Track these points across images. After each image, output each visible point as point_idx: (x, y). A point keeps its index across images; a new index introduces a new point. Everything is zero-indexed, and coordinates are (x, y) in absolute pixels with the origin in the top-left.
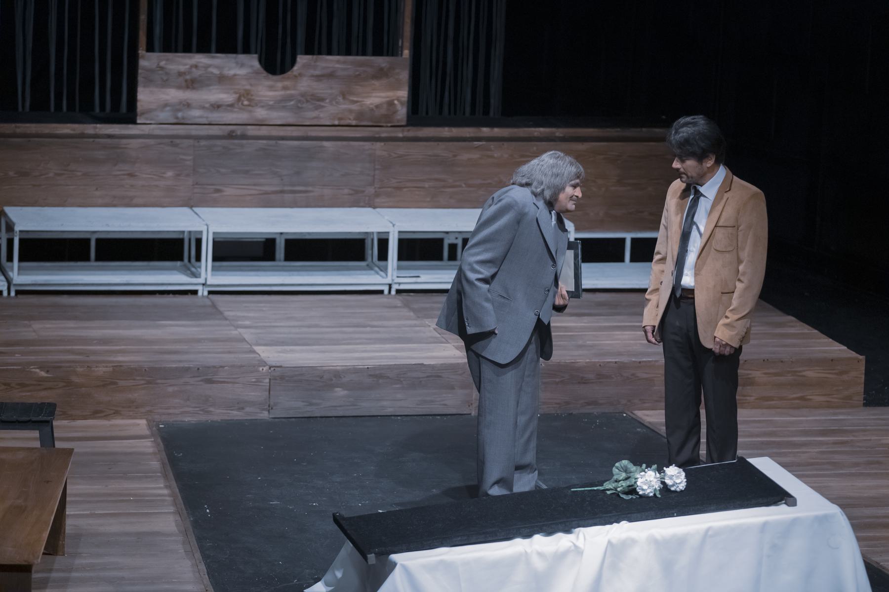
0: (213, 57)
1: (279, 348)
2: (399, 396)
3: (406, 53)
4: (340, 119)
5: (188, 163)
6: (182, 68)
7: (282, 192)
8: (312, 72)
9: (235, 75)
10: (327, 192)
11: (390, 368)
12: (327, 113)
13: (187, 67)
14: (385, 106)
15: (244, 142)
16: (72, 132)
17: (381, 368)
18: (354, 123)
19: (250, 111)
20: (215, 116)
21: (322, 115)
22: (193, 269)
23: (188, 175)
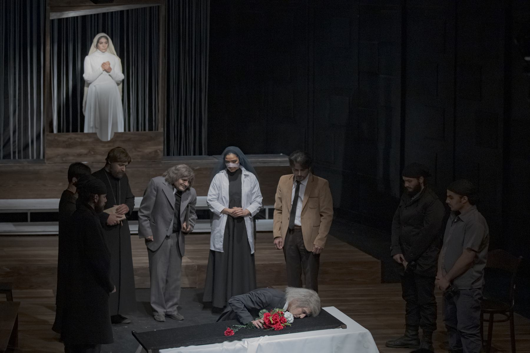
3: (161, 130)
18: (140, 160)
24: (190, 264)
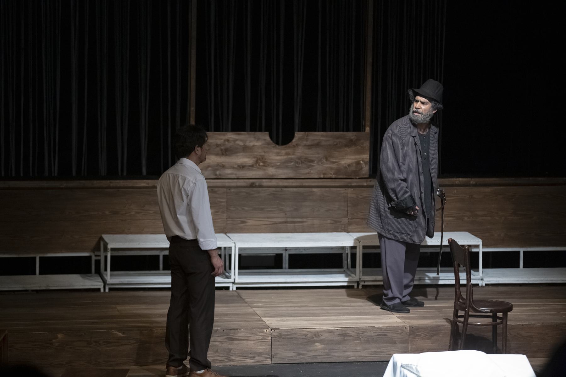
0: (239, 134)
1: (279, 319)
2: (359, 349)
3: (368, 129)
4: (324, 174)
5: (223, 204)
6: (219, 142)
7: (286, 222)
8: (305, 143)
9: (254, 146)
10: (316, 222)
11: (352, 329)
12: (316, 170)
13: (222, 141)
14: (354, 165)
15: (260, 189)
16: (147, 185)
17: (346, 329)
18: (334, 176)
19: (264, 170)
20: (241, 174)
21: (312, 172)
22: (227, 274)
23: (223, 212)
24: (400, 325)
